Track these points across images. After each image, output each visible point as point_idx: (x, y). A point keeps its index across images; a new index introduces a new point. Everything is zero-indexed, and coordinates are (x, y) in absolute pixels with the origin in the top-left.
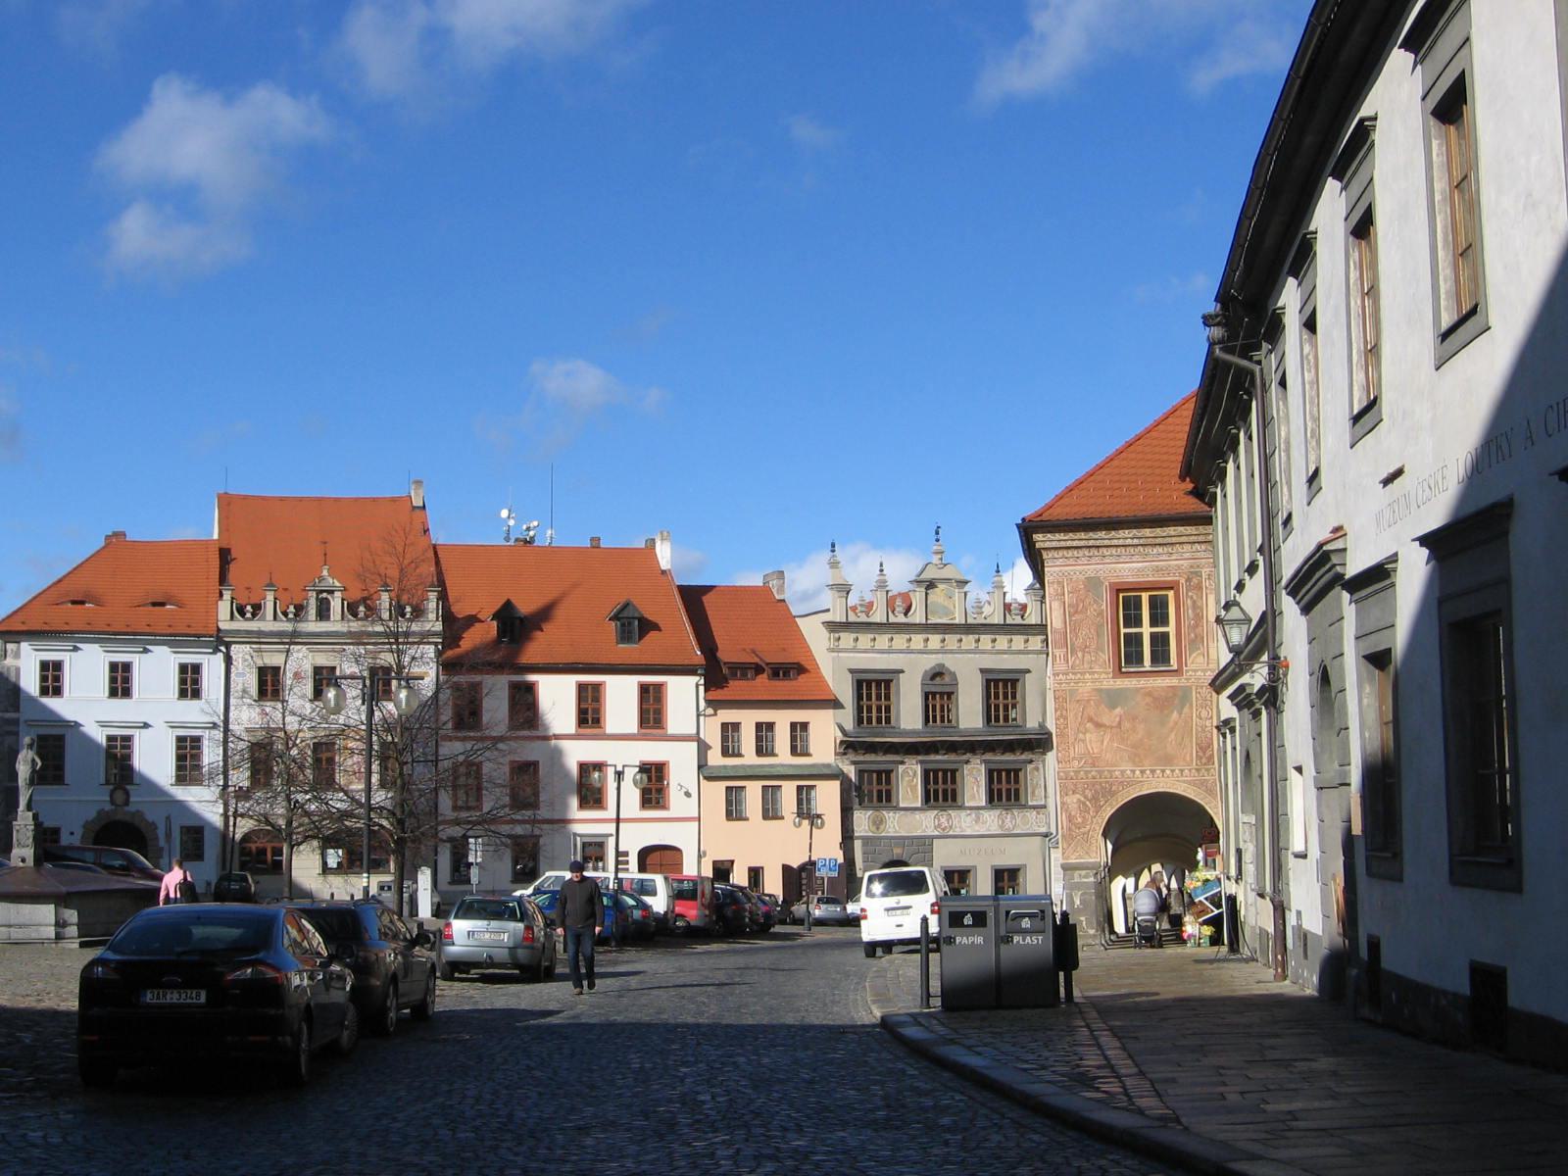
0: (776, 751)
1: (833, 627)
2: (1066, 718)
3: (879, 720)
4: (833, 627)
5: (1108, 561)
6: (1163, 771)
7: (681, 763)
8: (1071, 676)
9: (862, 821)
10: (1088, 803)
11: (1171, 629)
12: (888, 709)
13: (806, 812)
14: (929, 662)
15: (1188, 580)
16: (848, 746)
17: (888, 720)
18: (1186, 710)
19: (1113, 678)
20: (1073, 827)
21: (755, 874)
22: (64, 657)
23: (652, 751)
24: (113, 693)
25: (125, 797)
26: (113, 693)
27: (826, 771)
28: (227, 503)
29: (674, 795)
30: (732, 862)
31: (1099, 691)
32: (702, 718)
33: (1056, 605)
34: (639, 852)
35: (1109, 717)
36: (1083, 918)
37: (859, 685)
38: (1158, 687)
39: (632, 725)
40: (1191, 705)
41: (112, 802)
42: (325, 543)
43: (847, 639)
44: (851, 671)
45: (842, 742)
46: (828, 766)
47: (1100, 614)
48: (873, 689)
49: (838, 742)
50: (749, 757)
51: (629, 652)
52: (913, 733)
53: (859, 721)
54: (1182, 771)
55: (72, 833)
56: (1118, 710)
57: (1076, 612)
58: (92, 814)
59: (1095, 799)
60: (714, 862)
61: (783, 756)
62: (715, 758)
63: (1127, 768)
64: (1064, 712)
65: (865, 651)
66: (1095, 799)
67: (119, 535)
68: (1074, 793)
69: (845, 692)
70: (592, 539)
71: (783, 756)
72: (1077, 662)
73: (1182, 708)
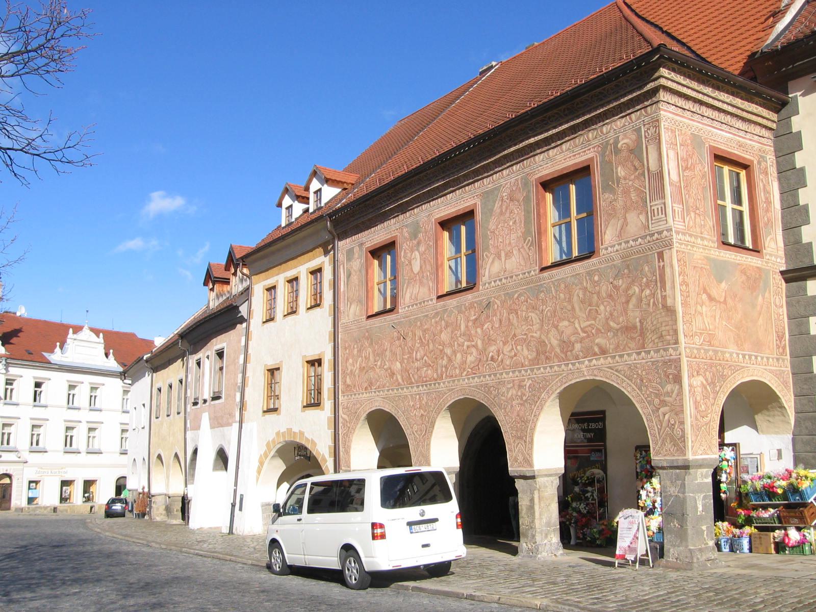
2: (687, 285)
5: (705, 122)
6: (756, 357)
8: (688, 238)
10: (708, 387)
11: (745, 208)
15: (759, 163)
18: (767, 295)
19: (718, 248)
20: (699, 417)
31: (707, 258)
33: (672, 154)
35: (719, 290)
36: (704, 528)
38: (750, 265)
40: (770, 292)
47: (704, 176)
54: (768, 358)
56: (723, 285)
57: (687, 168)
59: (712, 383)
63: (732, 348)
64: (686, 278)
66: (712, 383)
68: (698, 374)
72: (691, 223)
73: (765, 291)
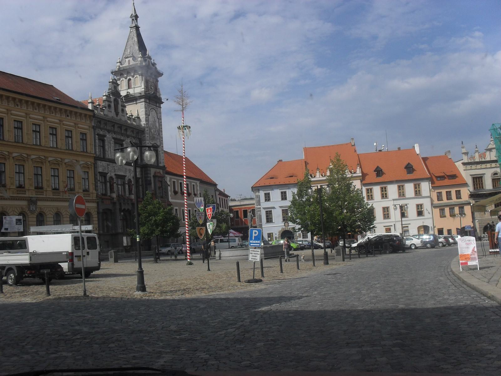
0: (452, 198)
1: (464, 164)
3: (480, 187)
4: (464, 164)
7: (427, 204)
9: (477, 214)
12: (482, 184)
13: (462, 213)
14: (493, 170)
16: (472, 196)
17: (482, 187)
21: (449, 231)
22: (270, 192)
23: (420, 201)
24: (282, 199)
25: (288, 224)
26: (282, 199)
27: (466, 202)
28: (306, 150)
29: (425, 213)
30: (443, 228)
32: (431, 192)
34: (418, 228)
37: (474, 178)
39: (413, 195)
41: (285, 225)
42: (330, 157)
43: (469, 167)
44: (471, 175)
45: (470, 194)
46: (467, 201)
48: (478, 180)
49: (469, 194)
50: (445, 201)
51: (410, 176)
52: (490, 190)
53: (475, 188)
55: (276, 234)
58: (280, 229)
60: (438, 229)
61: (454, 199)
62: (436, 202)
65: (474, 169)
67: (280, 161)
69: (470, 181)
70: (398, 148)
71: (454, 199)
